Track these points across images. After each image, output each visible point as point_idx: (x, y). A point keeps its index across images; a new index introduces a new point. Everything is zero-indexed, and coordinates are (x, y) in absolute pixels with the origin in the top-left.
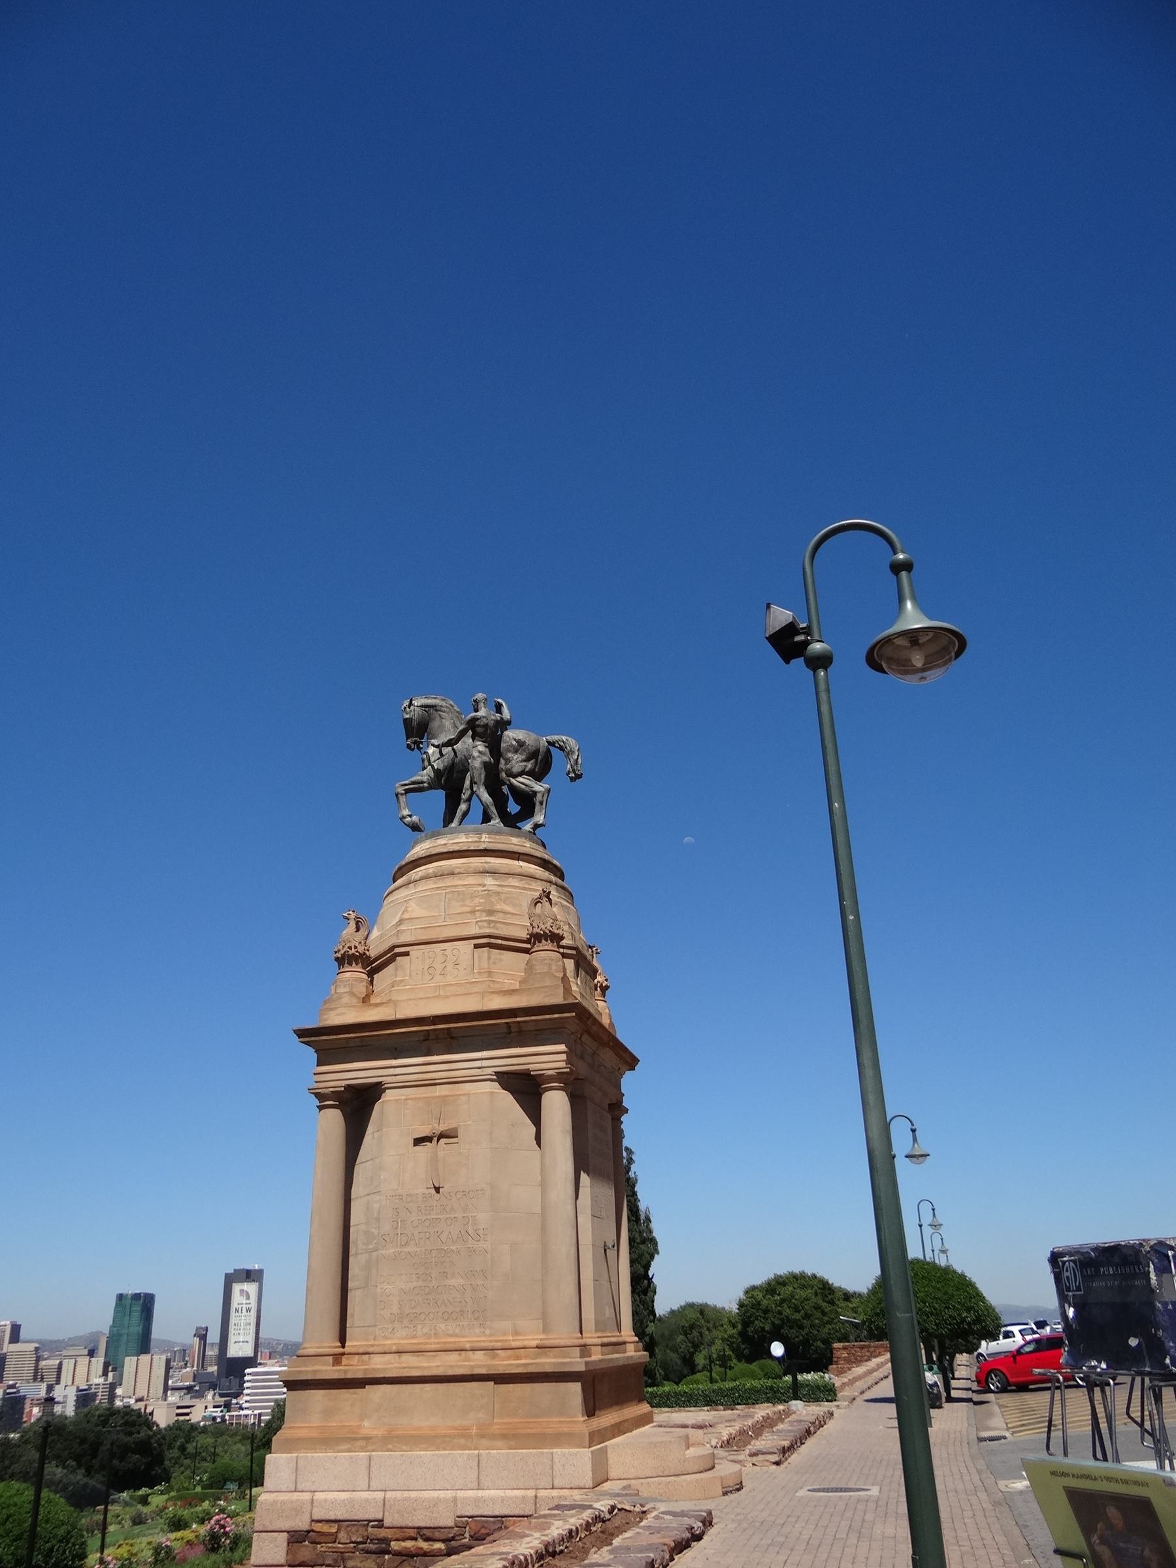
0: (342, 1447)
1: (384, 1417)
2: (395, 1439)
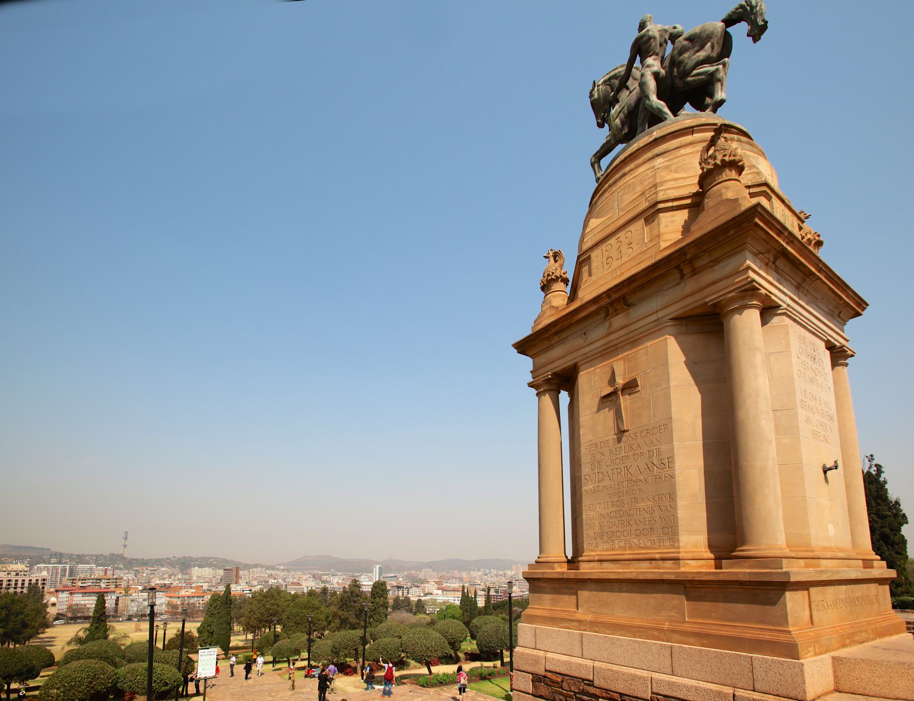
0: (563, 625)
1: (592, 607)
2: (600, 624)
